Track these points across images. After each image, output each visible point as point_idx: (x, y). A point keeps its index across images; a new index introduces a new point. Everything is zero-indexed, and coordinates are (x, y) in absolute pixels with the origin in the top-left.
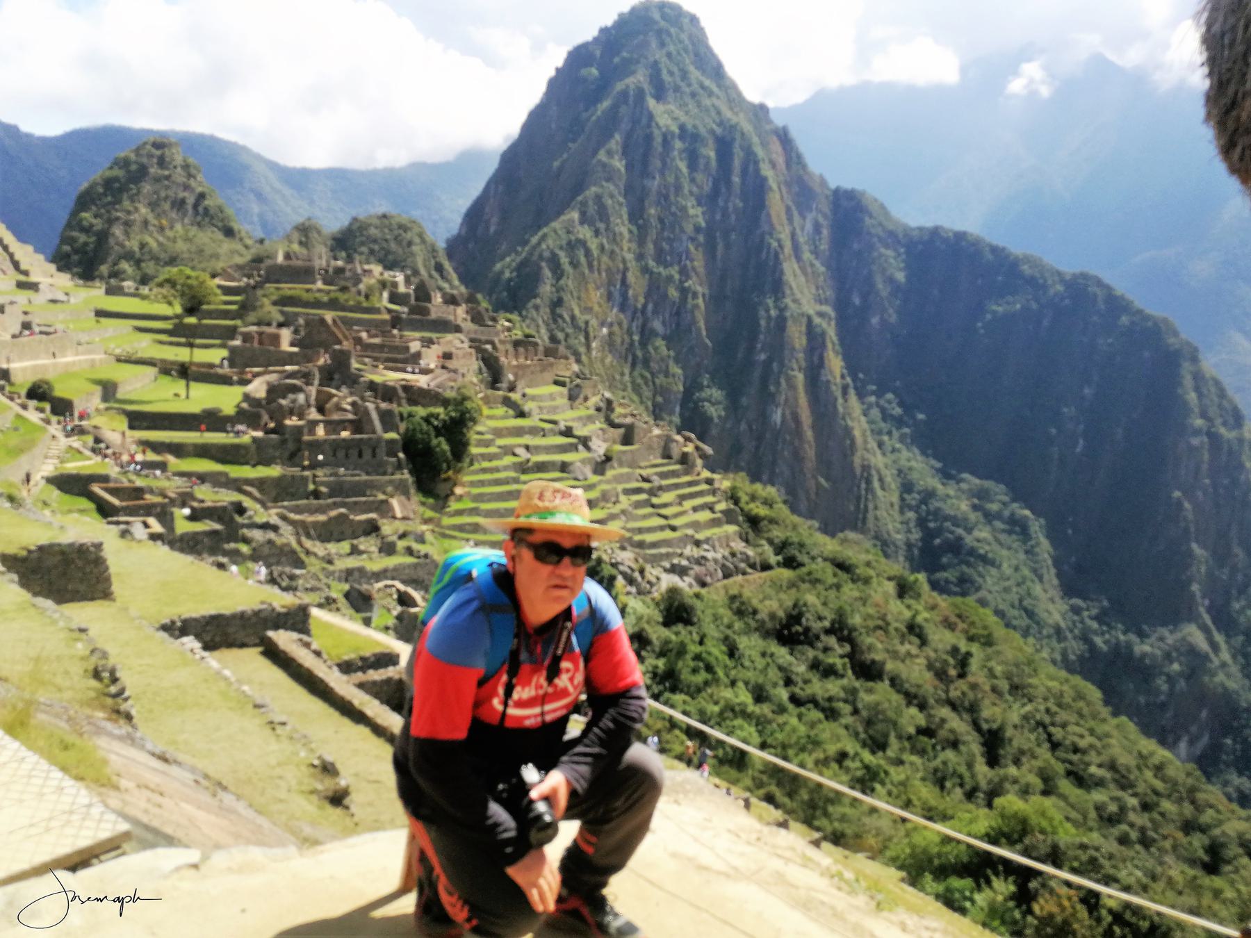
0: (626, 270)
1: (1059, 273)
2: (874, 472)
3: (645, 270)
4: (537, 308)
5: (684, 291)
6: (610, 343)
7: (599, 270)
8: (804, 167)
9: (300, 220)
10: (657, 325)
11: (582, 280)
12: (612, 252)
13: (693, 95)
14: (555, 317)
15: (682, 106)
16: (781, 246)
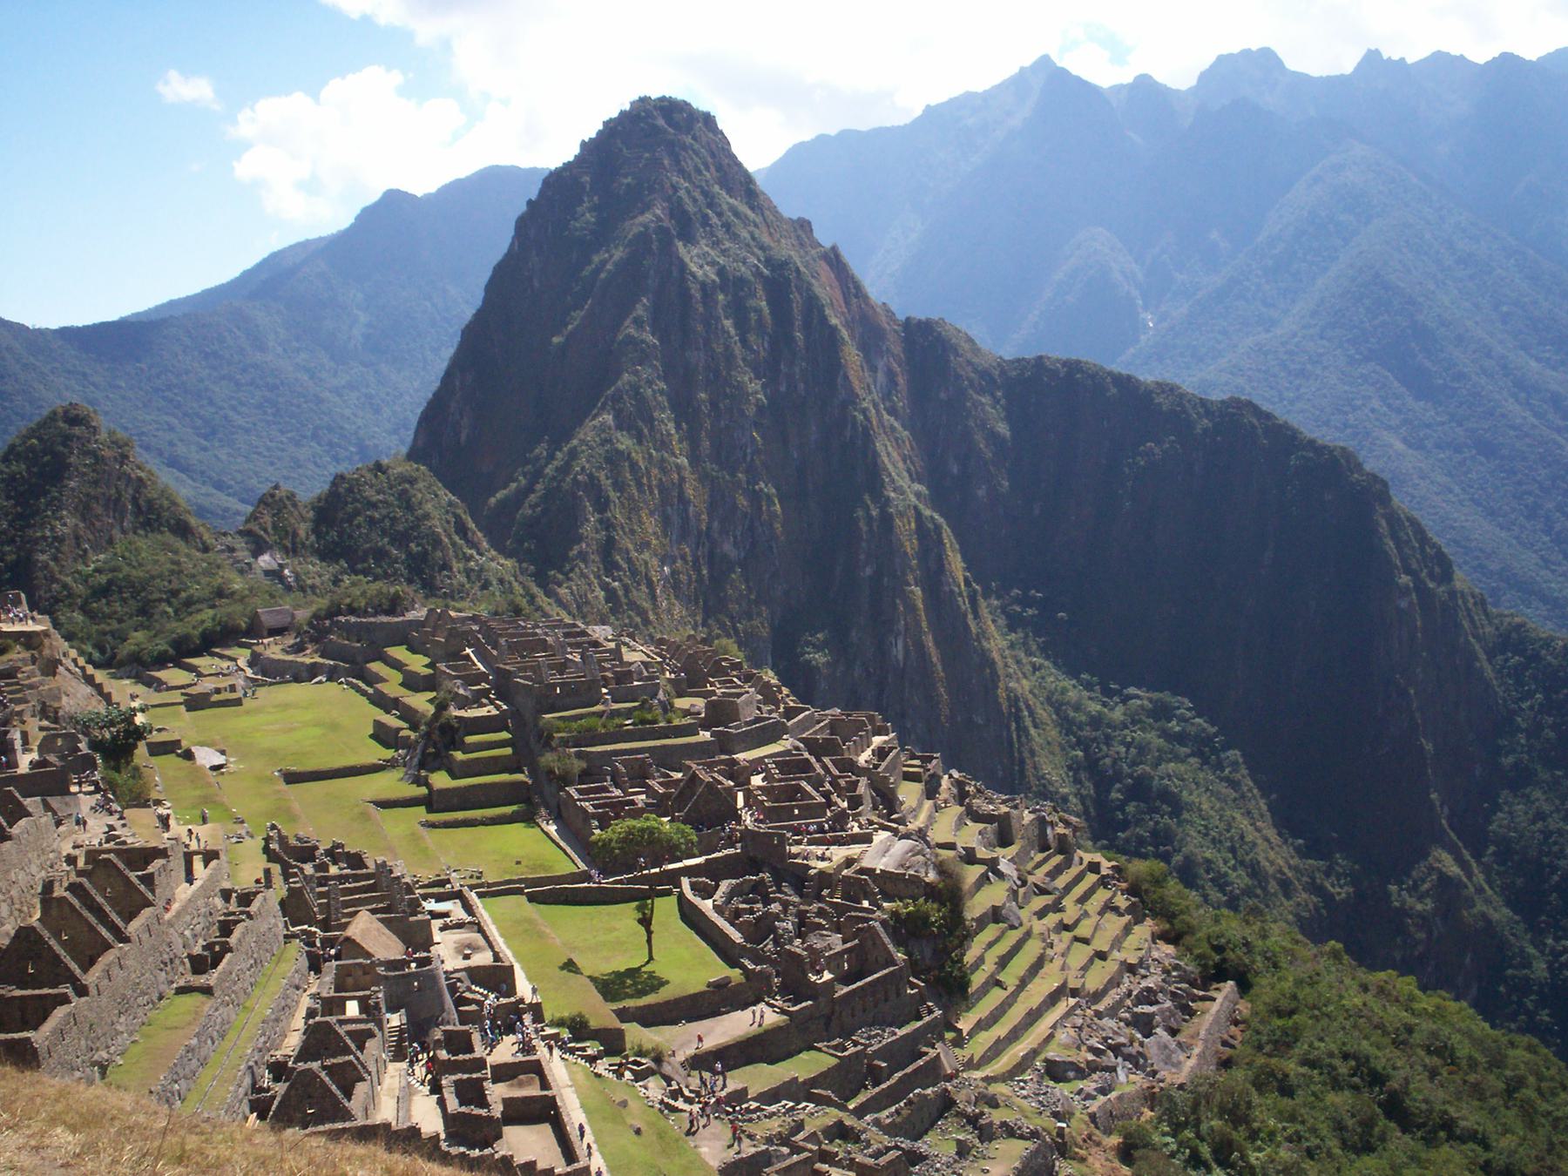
0: (682, 480)
1: (1203, 402)
2: (1021, 704)
3: (704, 478)
4: (583, 556)
5: (755, 497)
6: (674, 584)
7: (650, 487)
8: (866, 298)
9: (265, 488)
10: (728, 548)
11: (633, 510)
12: (663, 460)
13: (727, 226)
14: (610, 567)
15: (716, 244)
16: (867, 419)
